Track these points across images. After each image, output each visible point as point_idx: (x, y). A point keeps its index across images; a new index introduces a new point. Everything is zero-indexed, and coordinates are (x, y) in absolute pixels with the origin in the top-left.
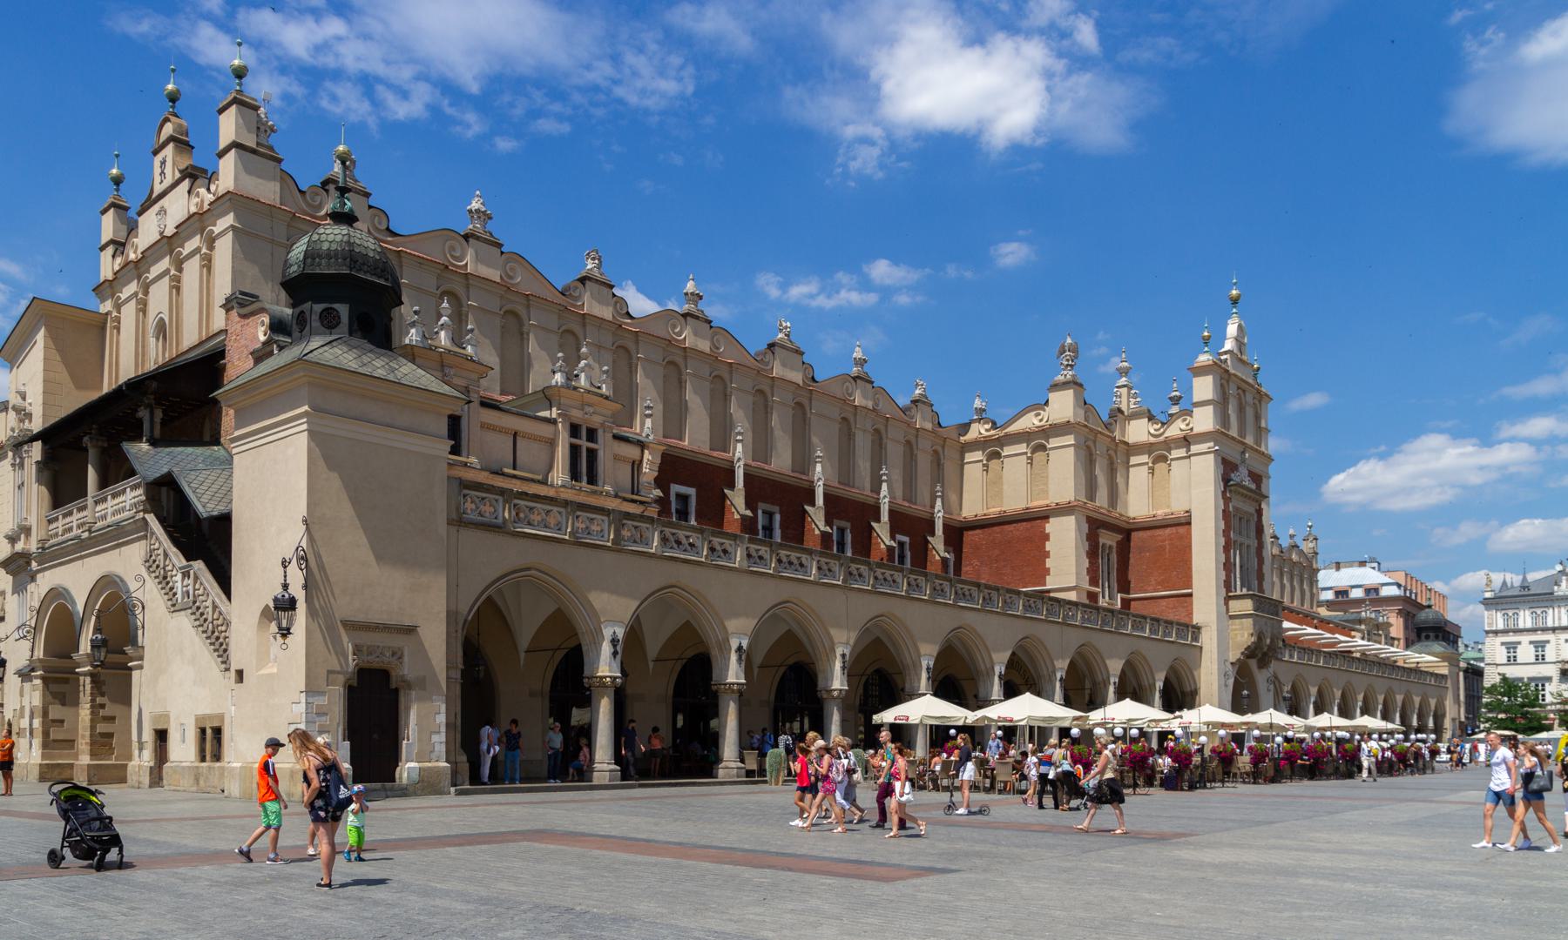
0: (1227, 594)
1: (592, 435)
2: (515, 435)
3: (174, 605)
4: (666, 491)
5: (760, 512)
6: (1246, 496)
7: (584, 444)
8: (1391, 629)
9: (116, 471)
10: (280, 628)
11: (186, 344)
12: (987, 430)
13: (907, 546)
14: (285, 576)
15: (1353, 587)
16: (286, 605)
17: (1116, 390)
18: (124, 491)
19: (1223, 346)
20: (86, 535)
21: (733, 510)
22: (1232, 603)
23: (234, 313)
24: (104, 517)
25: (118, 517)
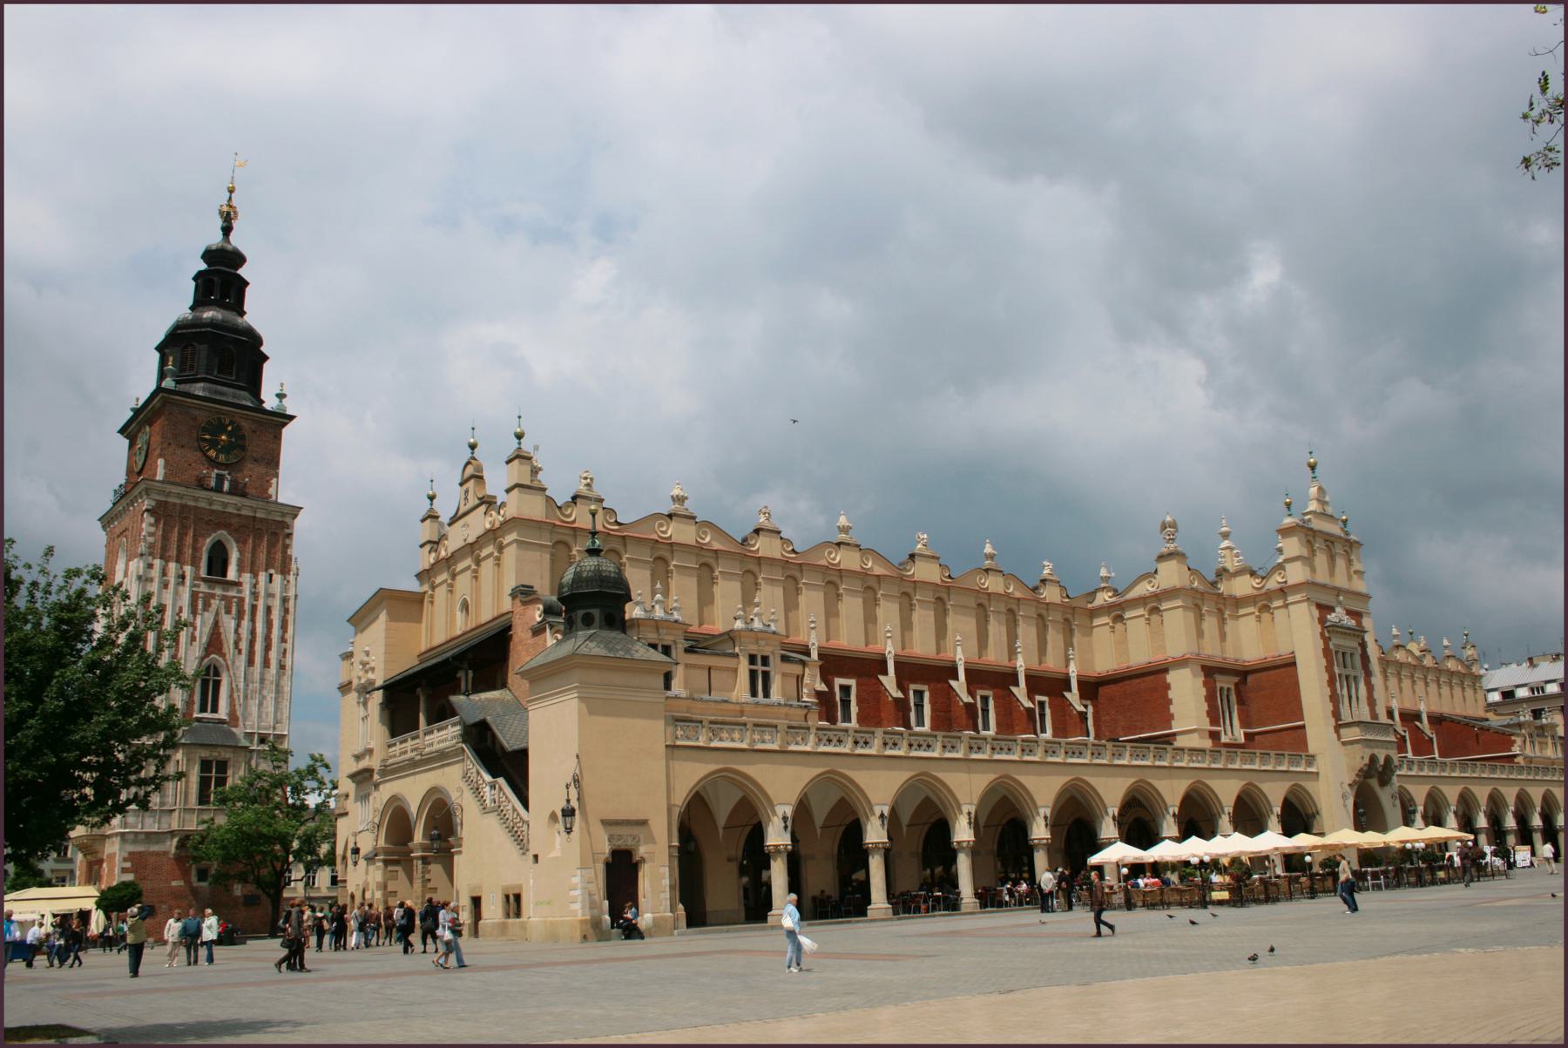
0: (1336, 721)
1: (765, 660)
2: (710, 669)
4: (830, 684)
5: (911, 693)
6: (1345, 633)
7: (760, 668)
8: (1558, 729)
9: (442, 713)
10: (566, 828)
12: (1110, 597)
13: (1047, 705)
15: (1518, 686)
16: (568, 813)
17: (1220, 551)
18: (446, 727)
20: (418, 757)
22: (1343, 731)
24: (431, 745)
25: (442, 745)
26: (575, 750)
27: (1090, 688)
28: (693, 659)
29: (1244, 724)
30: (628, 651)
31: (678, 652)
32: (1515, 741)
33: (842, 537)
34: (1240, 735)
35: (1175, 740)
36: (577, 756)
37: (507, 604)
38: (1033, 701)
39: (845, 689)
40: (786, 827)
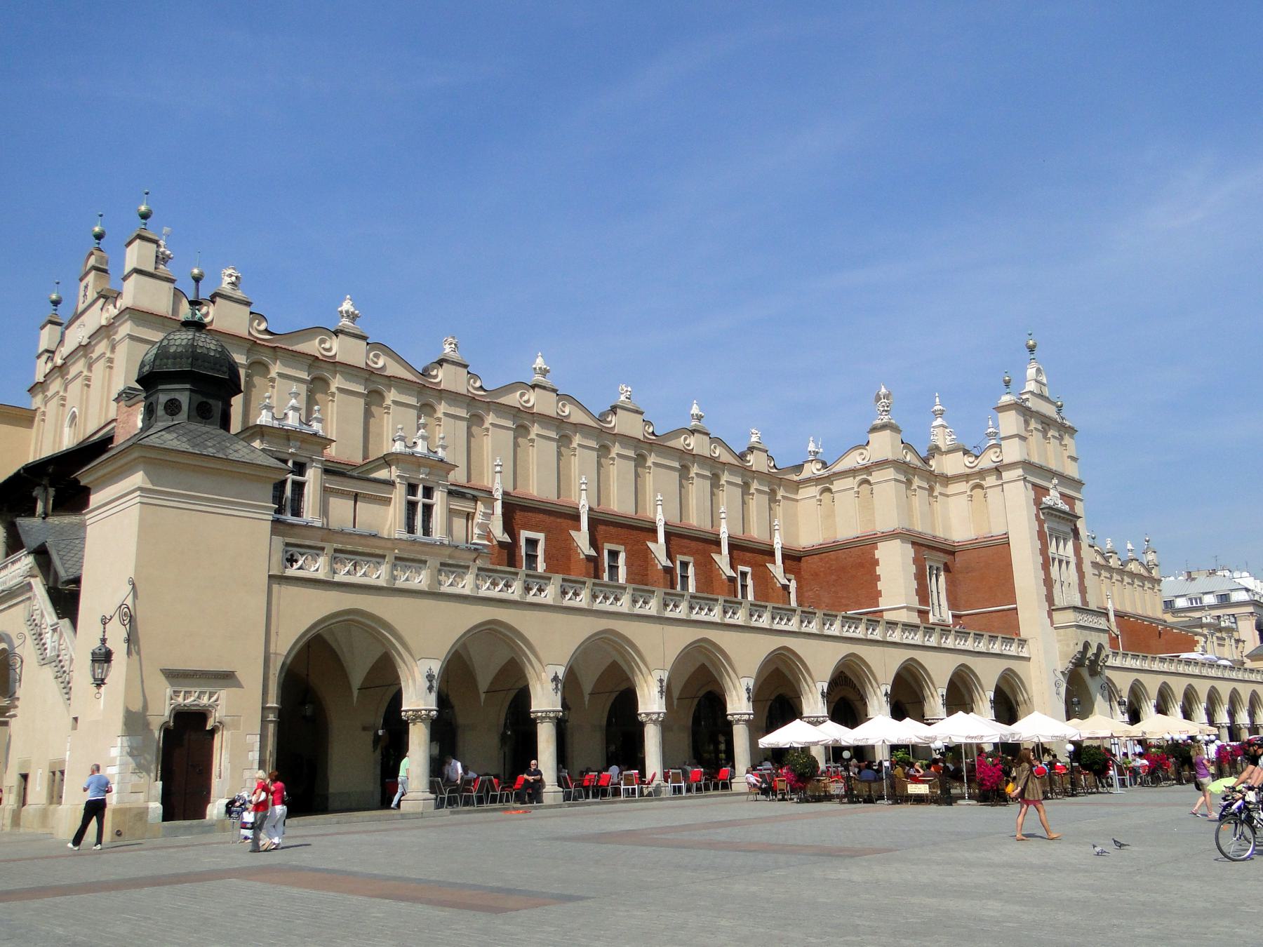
0: (1050, 607)
1: (428, 492)
3: (43, 659)
10: (95, 679)
11: (90, 431)
12: (818, 470)
13: (749, 576)
14: (104, 632)
17: (932, 429)
18: (19, 559)
21: (579, 551)
23: (122, 403)
26: (131, 573)
29: (952, 606)
30: (224, 449)
32: (1197, 642)
33: (538, 378)
34: (948, 616)
38: (735, 571)
39: (532, 543)
40: (430, 689)
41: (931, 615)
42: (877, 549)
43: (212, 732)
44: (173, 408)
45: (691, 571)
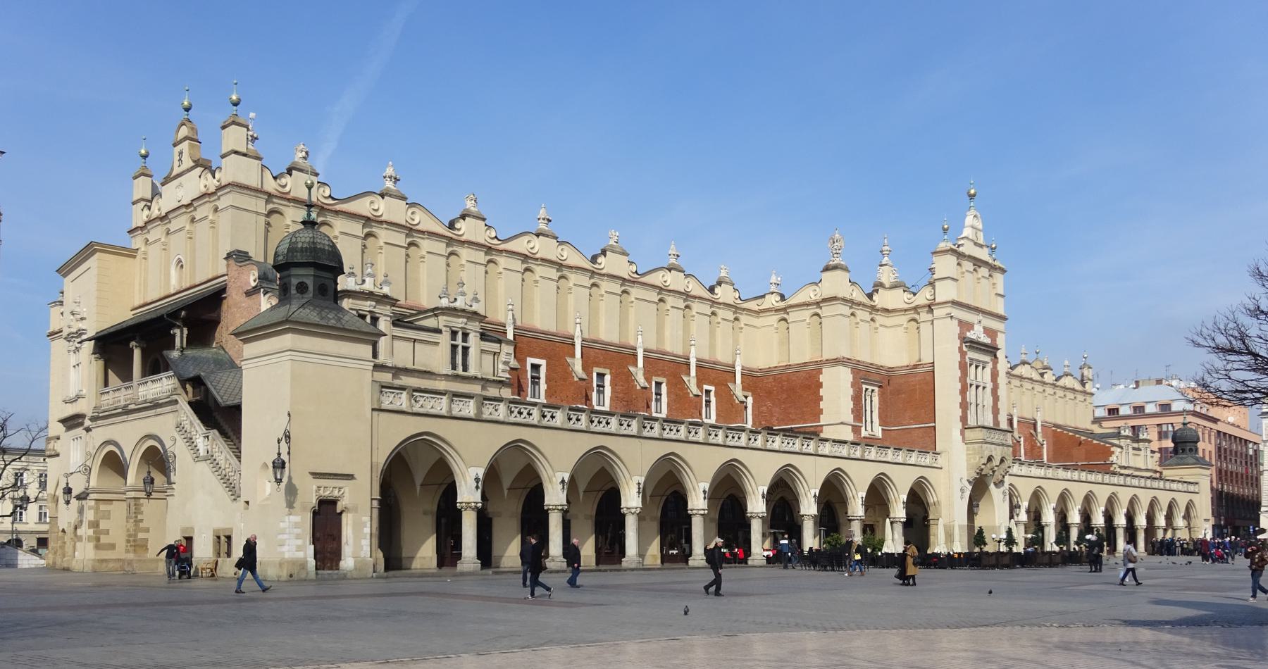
0: (963, 425)
1: (465, 336)
4: (522, 361)
10: (276, 479)
13: (712, 394)
19: (962, 233)
21: (574, 375)
26: (287, 408)
27: (753, 380)
28: (400, 332)
29: (883, 422)
31: (383, 325)
32: (1113, 452)
33: (542, 226)
34: (878, 432)
35: (822, 431)
36: (289, 415)
37: (222, 267)
39: (536, 367)
40: (477, 487)
41: (863, 429)
42: (822, 373)
43: (341, 514)
44: (302, 288)
45: (664, 388)
